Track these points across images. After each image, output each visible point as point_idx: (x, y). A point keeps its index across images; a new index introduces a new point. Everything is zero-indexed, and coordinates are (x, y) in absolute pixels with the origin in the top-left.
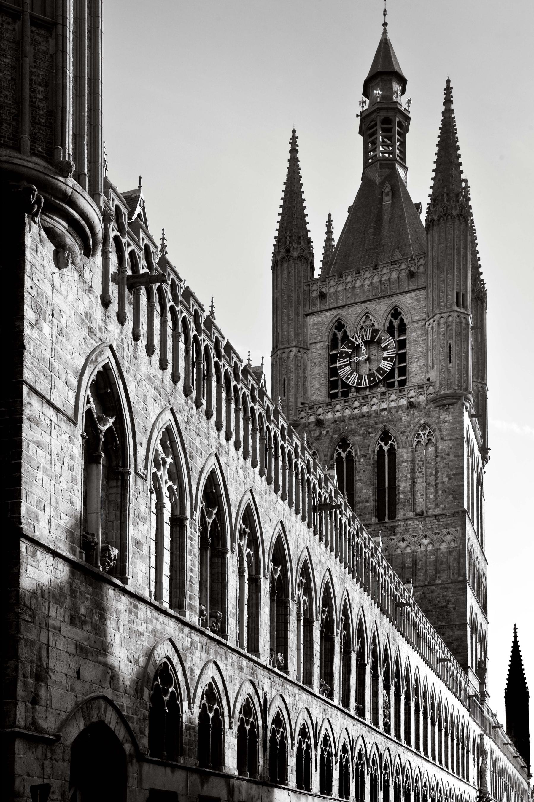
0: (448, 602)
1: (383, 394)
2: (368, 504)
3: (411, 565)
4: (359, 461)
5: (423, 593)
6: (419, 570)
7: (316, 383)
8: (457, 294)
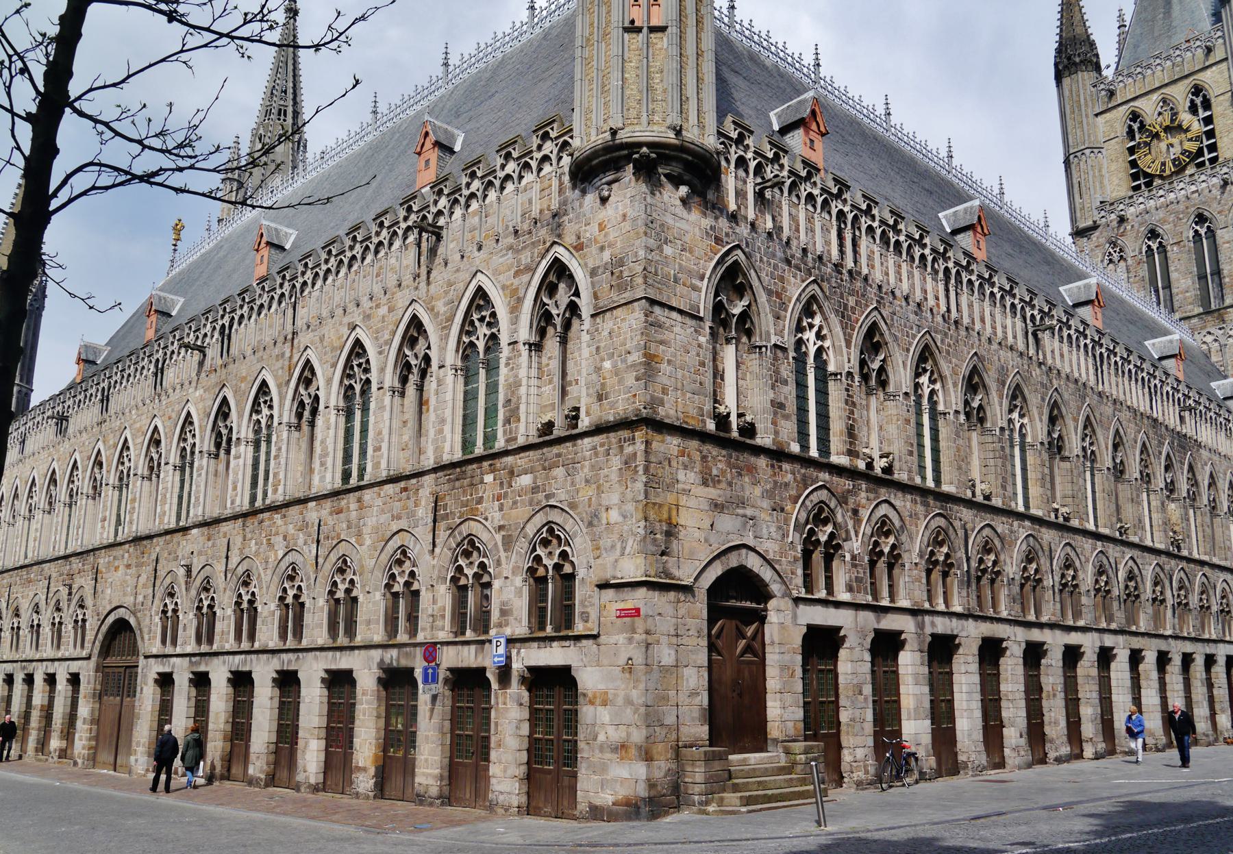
1: (1191, 176)
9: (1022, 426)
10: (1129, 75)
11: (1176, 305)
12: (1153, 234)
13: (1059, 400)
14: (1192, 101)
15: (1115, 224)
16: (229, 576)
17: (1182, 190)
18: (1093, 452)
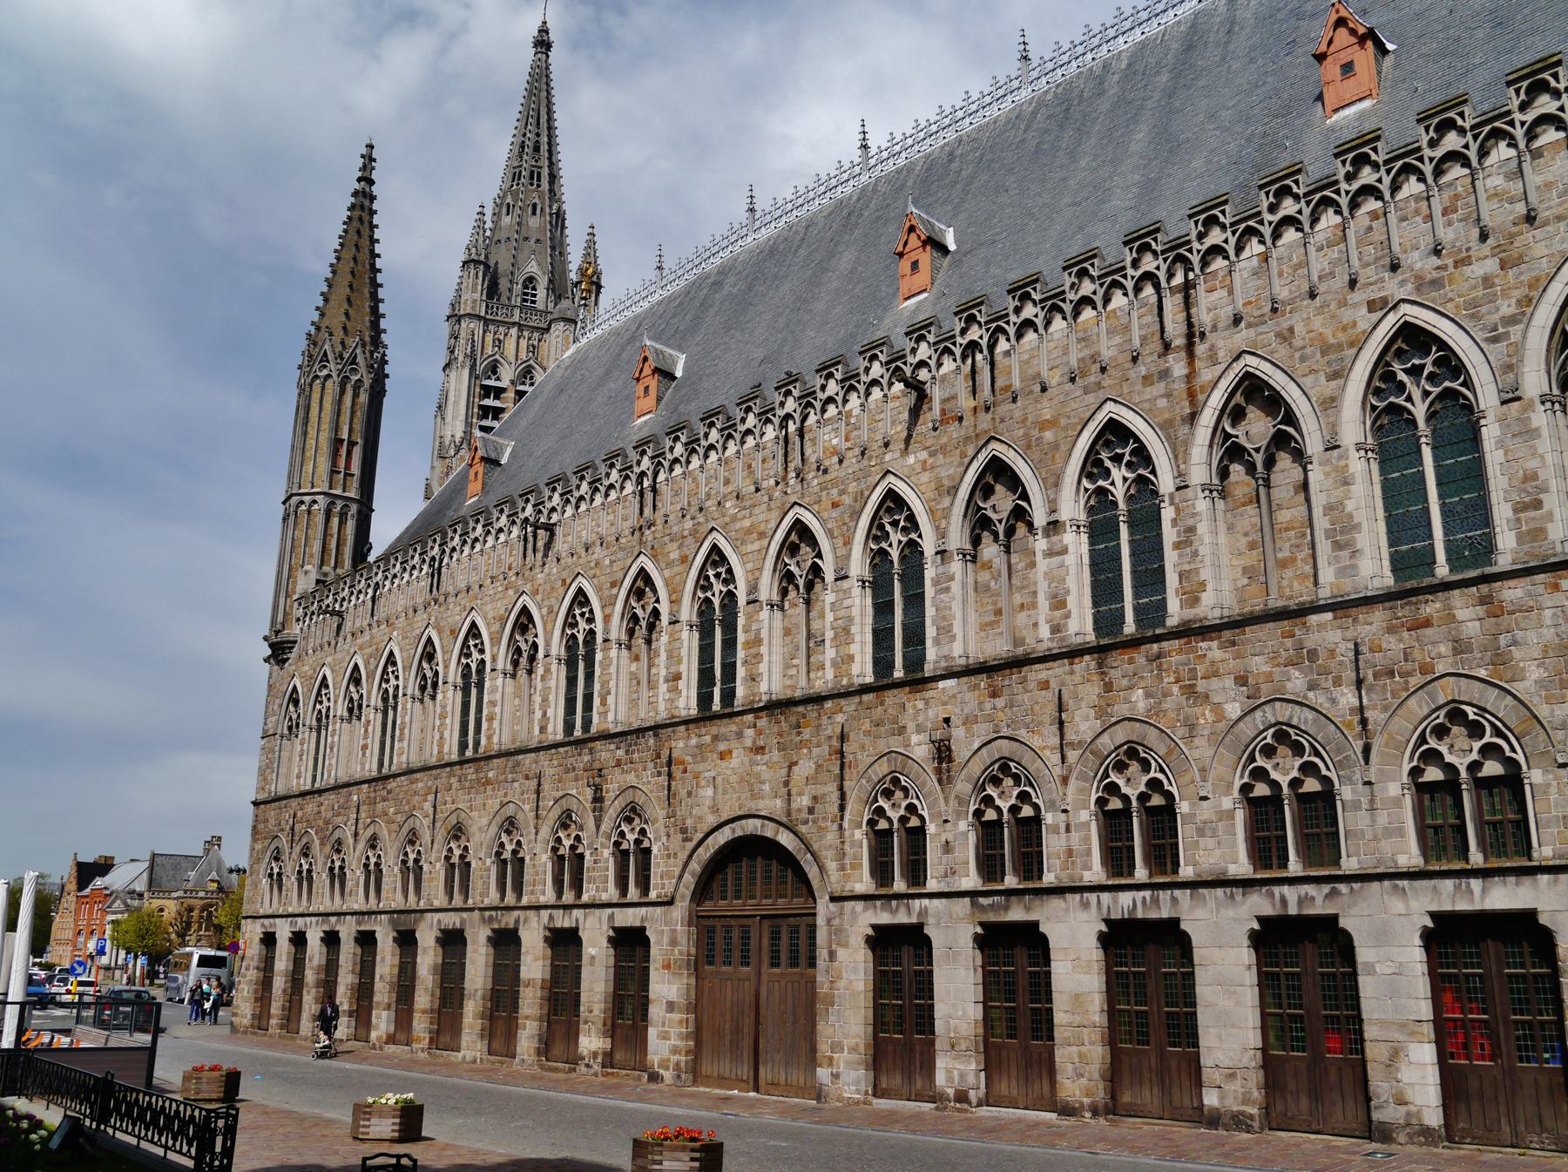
16: (1073, 756)
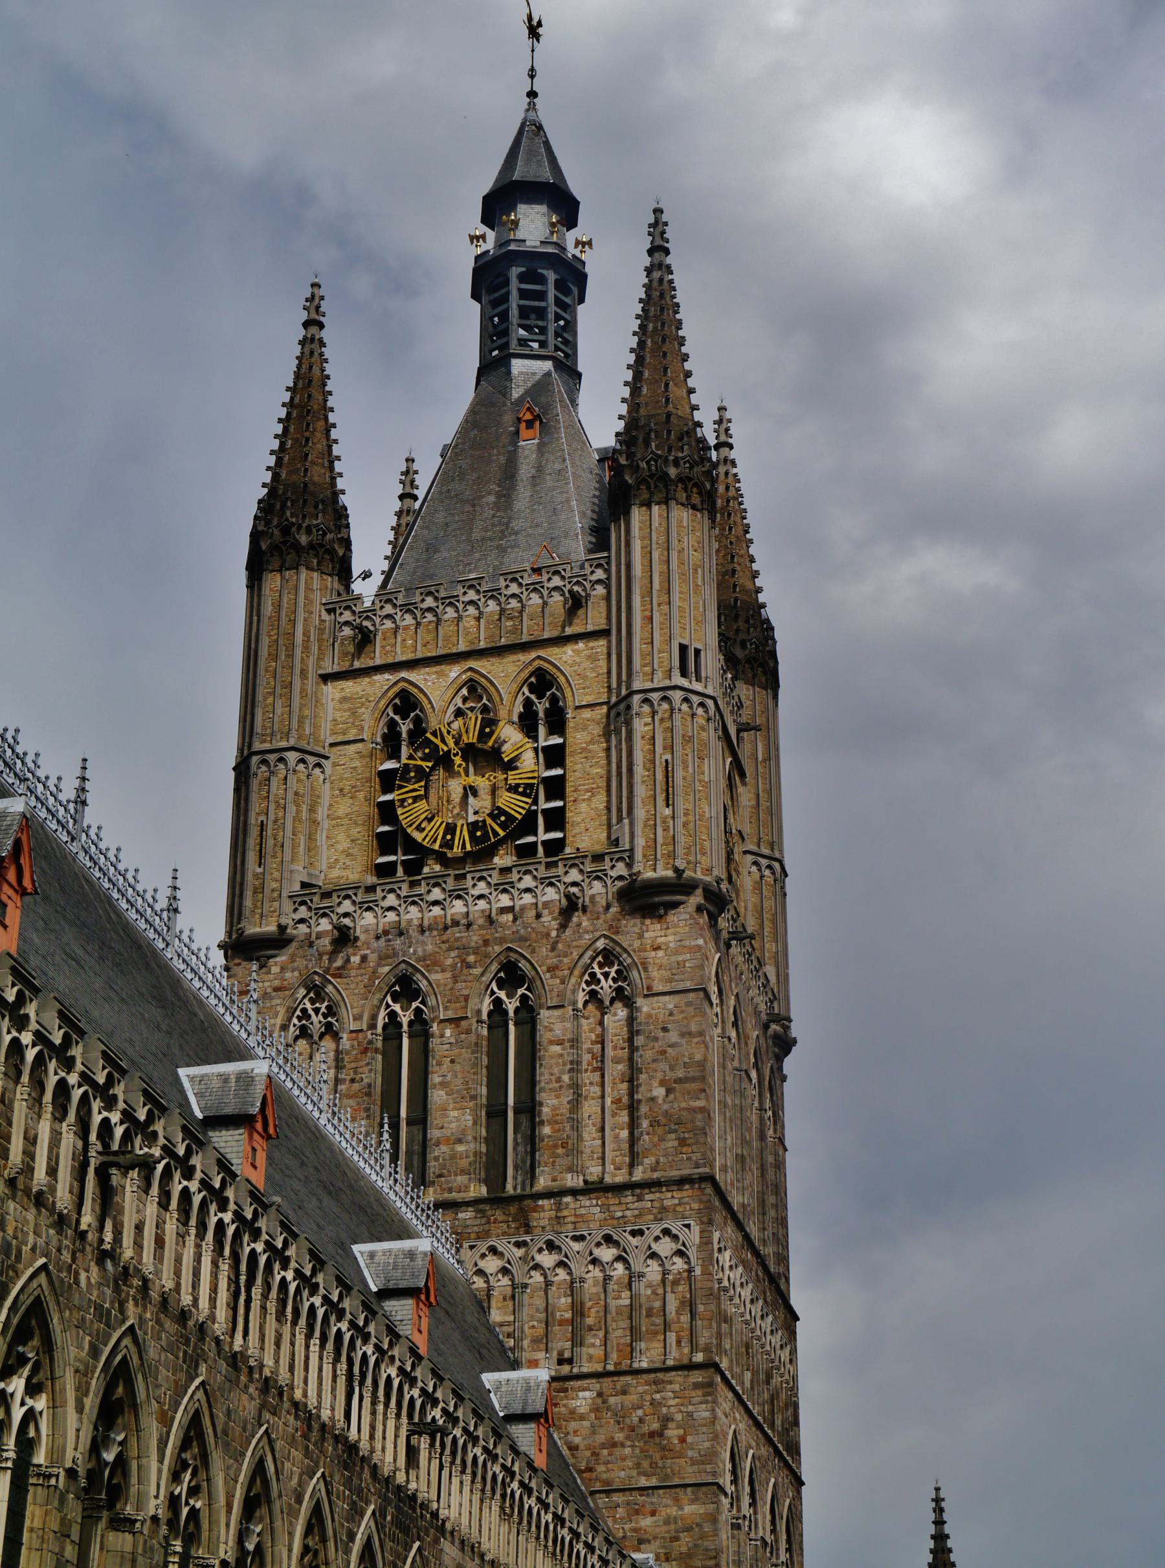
0: (666, 1420)
1: (505, 870)
2: (460, 1148)
3: (568, 1315)
4: (442, 1036)
5: (600, 1394)
6: (590, 1329)
7: (341, 837)
8: (683, 649)
9: (30, 1416)
10: (408, 608)
11: (433, 1167)
12: (406, 988)
13: (135, 1360)
14: (528, 703)
15: (325, 943)
17: (481, 899)
18: (194, 1513)
